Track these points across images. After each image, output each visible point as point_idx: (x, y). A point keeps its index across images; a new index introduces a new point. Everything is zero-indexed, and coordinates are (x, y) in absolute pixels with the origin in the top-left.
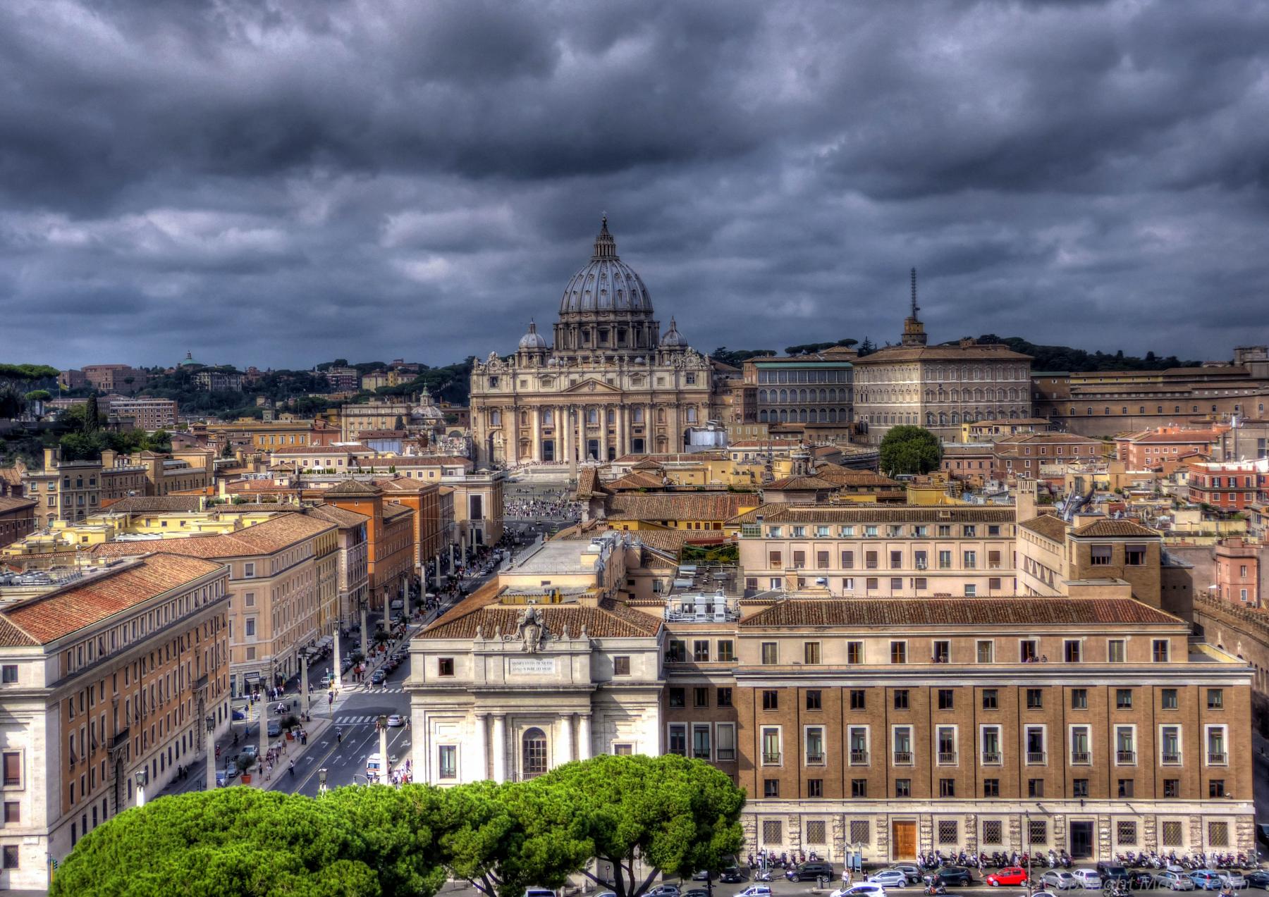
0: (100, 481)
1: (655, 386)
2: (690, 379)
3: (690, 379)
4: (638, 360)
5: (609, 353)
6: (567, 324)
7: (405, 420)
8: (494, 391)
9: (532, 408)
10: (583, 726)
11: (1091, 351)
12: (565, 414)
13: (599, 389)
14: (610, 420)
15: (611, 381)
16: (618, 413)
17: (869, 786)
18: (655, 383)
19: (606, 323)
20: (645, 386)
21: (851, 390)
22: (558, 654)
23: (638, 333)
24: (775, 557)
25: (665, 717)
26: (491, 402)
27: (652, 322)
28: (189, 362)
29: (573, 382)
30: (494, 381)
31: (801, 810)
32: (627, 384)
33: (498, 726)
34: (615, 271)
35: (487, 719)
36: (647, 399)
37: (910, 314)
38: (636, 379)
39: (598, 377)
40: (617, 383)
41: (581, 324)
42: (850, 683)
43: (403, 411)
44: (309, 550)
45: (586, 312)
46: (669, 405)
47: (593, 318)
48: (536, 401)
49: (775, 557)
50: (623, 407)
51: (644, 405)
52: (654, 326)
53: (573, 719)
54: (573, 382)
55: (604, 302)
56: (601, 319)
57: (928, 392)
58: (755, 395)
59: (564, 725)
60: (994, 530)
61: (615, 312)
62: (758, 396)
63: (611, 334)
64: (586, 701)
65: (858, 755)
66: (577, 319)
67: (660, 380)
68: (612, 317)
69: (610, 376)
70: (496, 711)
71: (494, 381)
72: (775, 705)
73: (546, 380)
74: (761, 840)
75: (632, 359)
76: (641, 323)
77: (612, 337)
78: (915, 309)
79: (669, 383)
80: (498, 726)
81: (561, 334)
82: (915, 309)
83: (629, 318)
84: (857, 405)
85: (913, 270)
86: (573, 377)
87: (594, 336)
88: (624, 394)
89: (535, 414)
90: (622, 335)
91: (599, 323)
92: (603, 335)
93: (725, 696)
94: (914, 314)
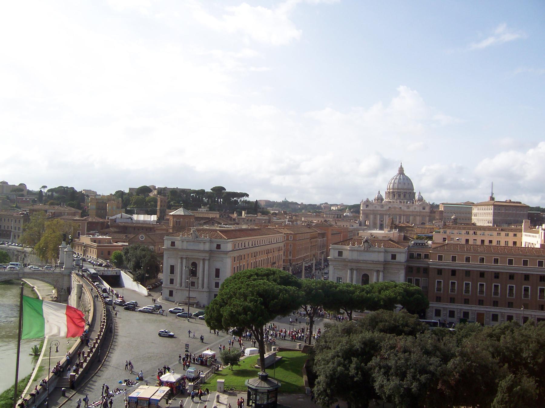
0: (256, 220)
2: (424, 209)
3: (424, 209)
6: (389, 192)
7: (342, 216)
10: (381, 275)
13: (397, 210)
14: (400, 219)
15: (401, 208)
16: (402, 217)
22: (375, 252)
25: (406, 275)
29: (390, 207)
30: (367, 206)
31: (447, 307)
32: (405, 209)
33: (355, 272)
35: (352, 270)
38: (408, 207)
39: (397, 206)
40: (402, 208)
41: (393, 192)
42: (466, 269)
44: (309, 236)
46: (417, 215)
48: (379, 212)
50: (404, 215)
51: (410, 215)
53: (378, 272)
54: (390, 207)
55: (400, 187)
59: (375, 274)
60: (515, 235)
61: (403, 189)
64: (382, 266)
65: (467, 291)
67: (415, 208)
68: (402, 191)
70: (354, 268)
72: (441, 274)
74: (434, 315)
75: (407, 203)
76: (410, 193)
77: (402, 196)
78: (492, 194)
79: (418, 209)
80: (355, 272)
82: (492, 194)
83: (407, 191)
86: (390, 206)
87: (396, 196)
88: (404, 211)
89: (379, 216)
90: (405, 196)
91: (398, 192)
92: (399, 196)
93: (426, 270)
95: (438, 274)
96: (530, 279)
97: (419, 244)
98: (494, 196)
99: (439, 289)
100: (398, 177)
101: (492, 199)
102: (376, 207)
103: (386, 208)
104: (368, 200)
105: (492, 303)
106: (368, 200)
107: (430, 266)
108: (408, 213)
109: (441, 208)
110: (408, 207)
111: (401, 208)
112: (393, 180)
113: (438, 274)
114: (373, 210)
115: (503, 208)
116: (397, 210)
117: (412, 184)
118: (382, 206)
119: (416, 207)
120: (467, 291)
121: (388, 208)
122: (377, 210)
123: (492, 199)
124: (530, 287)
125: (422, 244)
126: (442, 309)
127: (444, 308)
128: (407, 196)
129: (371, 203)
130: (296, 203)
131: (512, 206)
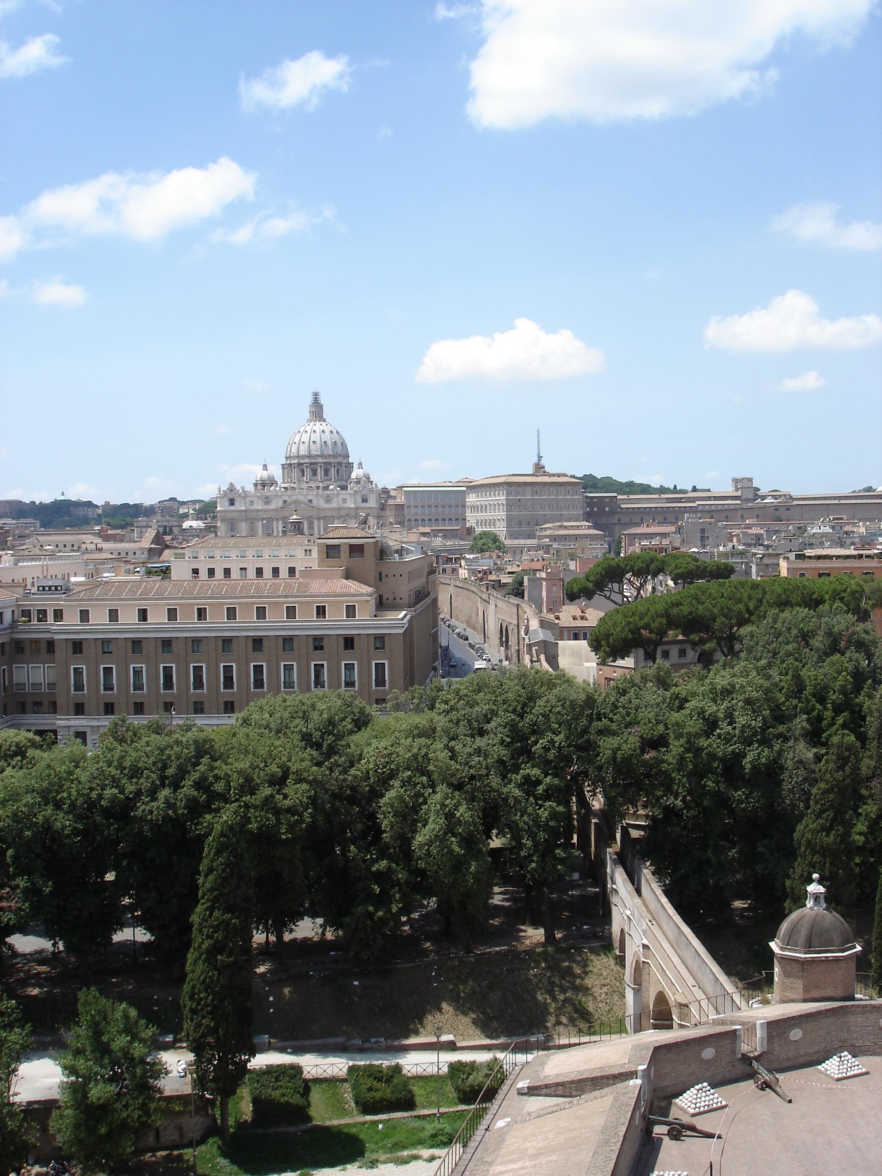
1: (341, 505)
2: (365, 500)
3: (365, 500)
4: (331, 487)
5: (317, 484)
6: (290, 465)
7: (176, 530)
8: (232, 508)
9: (258, 520)
11: (655, 485)
12: (280, 523)
15: (310, 501)
16: (316, 522)
17: (146, 707)
18: (341, 502)
19: (316, 464)
20: (334, 505)
21: (464, 506)
23: (338, 470)
24: (196, 571)
26: (229, 515)
27: (349, 463)
28: (62, 498)
29: (285, 502)
30: (232, 502)
31: (99, 724)
34: (322, 428)
36: (335, 513)
37: (536, 461)
38: (328, 500)
39: (301, 498)
40: (315, 502)
41: (299, 464)
42: (131, 636)
43: (175, 524)
45: (303, 457)
47: (307, 461)
49: (196, 571)
50: (319, 519)
52: (350, 466)
54: (285, 502)
56: (314, 461)
57: (510, 505)
58: (403, 509)
62: (405, 509)
63: (319, 471)
65: (138, 687)
66: (296, 461)
67: (344, 500)
68: (320, 460)
69: (310, 498)
71: (232, 502)
73: (267, 500)
76: (340, 464)
78: (540, 457)
81: (286, 470)
82: (540, 457)
84: (469, 514)
85: (538, 431)
87: (308, 472)
88: (319, 509)
91: (311, 464)
92: (314, 473)
93: (51, 645)
94: (539, 460)
95: (75, 652)
96: (264, 649)
97: (50, 587)
98: (542, 463)
99: (79, 687)
100: (309, 429)
101: (539, 468)
102: (252, 502)
103: (276, 504)
104: (232, 488)
105: (192, 707)
106: (232, 488)
107: (56, 637)
108: (330, 514)
109: (401, 500)
110: (328, 500)
111: (310, 501)
112: (298, 436)
113: (75, 652)
114: (246, 511)
115: (529, 488)
116: (302, 505)
117: (343, 444)
118: (267, 500)
119: (348, 497)
120: (138, 687)
121: (280, 504)
122: (257, 511)
123: (539, 468)
124: (204, 665)
125: (56, 587)
126: (88, 730)
127: (92, 727)
128: (333, 471)
129: (245, 495)
130: (89, 504)
131: (545, 484)
